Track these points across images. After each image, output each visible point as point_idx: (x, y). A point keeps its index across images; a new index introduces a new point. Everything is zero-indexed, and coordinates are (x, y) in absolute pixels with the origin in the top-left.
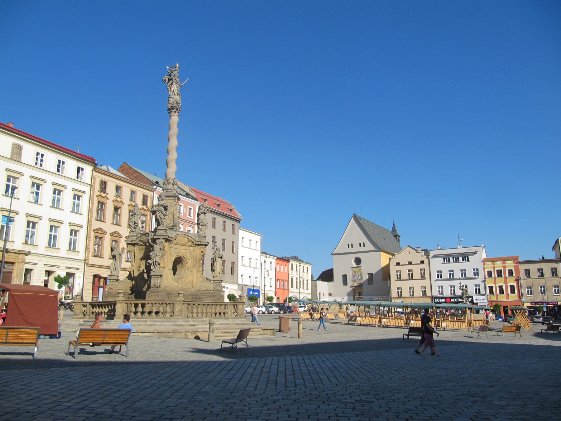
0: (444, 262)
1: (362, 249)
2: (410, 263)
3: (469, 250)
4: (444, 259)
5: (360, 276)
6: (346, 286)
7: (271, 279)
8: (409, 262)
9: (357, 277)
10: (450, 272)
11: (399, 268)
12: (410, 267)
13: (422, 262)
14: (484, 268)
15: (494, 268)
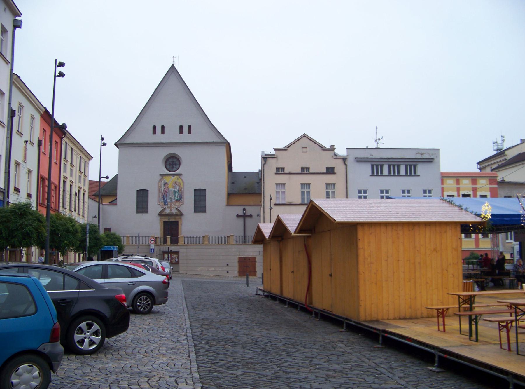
0: (373, 172)
1: (185, 137)
2: (305, 171)
3: (418, 153)
4: (373, 167)
5: (177, 194)
6: (145, 215)
7: (30, 172)
8: (303, 169)
9: (170, 195)
10: (361, 193)
11: (281, 179)
12: (306, 179)
13: (330, 171)
14: (443, 190)
15: (458, 190)
